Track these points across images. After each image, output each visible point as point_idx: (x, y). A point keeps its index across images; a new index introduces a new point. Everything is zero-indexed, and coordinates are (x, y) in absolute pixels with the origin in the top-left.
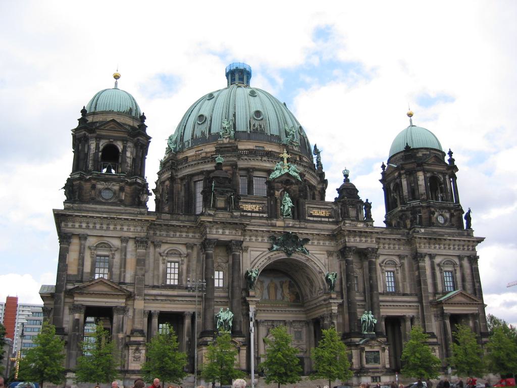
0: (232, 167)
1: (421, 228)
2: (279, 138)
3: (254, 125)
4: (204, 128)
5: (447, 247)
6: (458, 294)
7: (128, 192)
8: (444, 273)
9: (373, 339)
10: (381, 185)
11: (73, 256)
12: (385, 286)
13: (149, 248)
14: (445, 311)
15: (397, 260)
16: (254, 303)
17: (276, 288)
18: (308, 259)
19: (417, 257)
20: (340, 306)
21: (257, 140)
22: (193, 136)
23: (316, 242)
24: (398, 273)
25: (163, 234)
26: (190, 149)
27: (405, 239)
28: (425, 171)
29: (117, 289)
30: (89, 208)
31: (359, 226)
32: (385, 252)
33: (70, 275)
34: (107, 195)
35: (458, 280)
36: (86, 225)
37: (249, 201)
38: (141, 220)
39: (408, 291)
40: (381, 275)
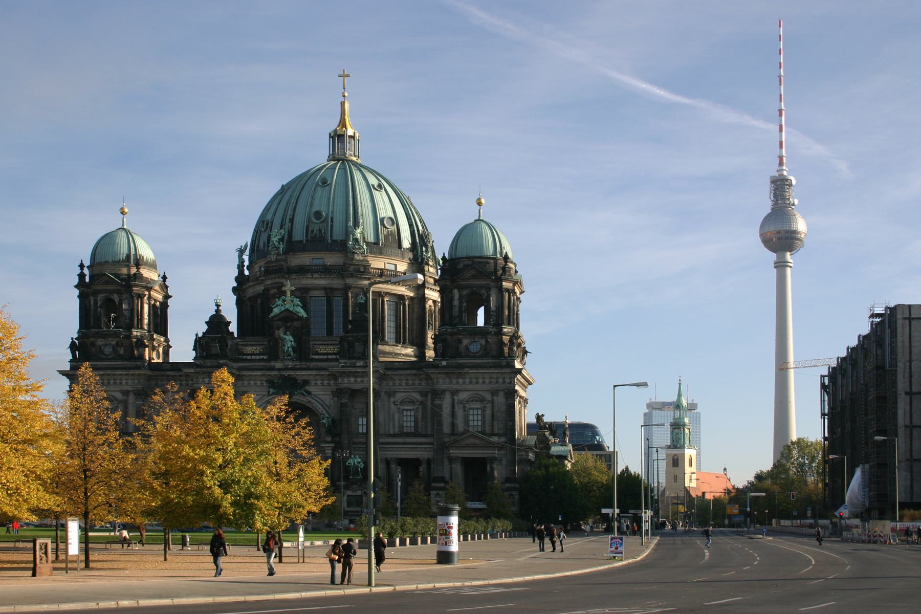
1: (442, 360)
3: (312, 231)
4: (264, 238)
5: (474, 381)
8: (471, 412)
14: (452, 455)
15: (417, 396)
18: (309, 402)
19: (437, 394)
21: (314, 251)
23: (319, 382)
24: (417, 412)
31: (358, 364)
34: (108, 350)
35: (487, 418)
37: (248, 343)
39: (429, 432)
40: (396, 416)
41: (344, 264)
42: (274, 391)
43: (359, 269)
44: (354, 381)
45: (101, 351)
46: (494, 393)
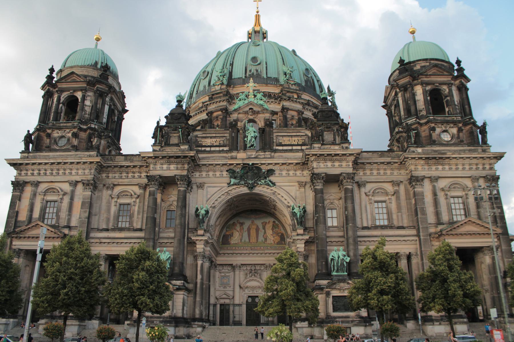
0: (222, 112)
1: (417, 147)
2: (277, 80)
3: (250, 71)
4: (206, 82)
5: (454, 167)
6: (465, 223)
7: (84, 138)
8: (452, 200)
9: (343, 281)
10: (385, 111)
11: (25, 203)
12: (374, 219)
13: (101, 191)
15: (389, 188)
16: (203, 242)
17: (257, 230)
18: (274, 193)
20: (307, 243)
22: (197, 91)
23: (284, 173)
24: (391, 203)
25: (115, 177)
26: (195, 103)
27: (397, 163)
28: (422, 84)
29: (52, 231)
30: (43, 156)
32: (372, 179)
33: (20, 221)
34: (62, 142)
36: (38, 172)
37: (208, 135)
38: (86, 162)
40: (368, 207)
41: (282, 91)
42: (237, 181)
43: (293, 97)
44: (332, 165)
45: (56, 143)
46: (474, 179)
